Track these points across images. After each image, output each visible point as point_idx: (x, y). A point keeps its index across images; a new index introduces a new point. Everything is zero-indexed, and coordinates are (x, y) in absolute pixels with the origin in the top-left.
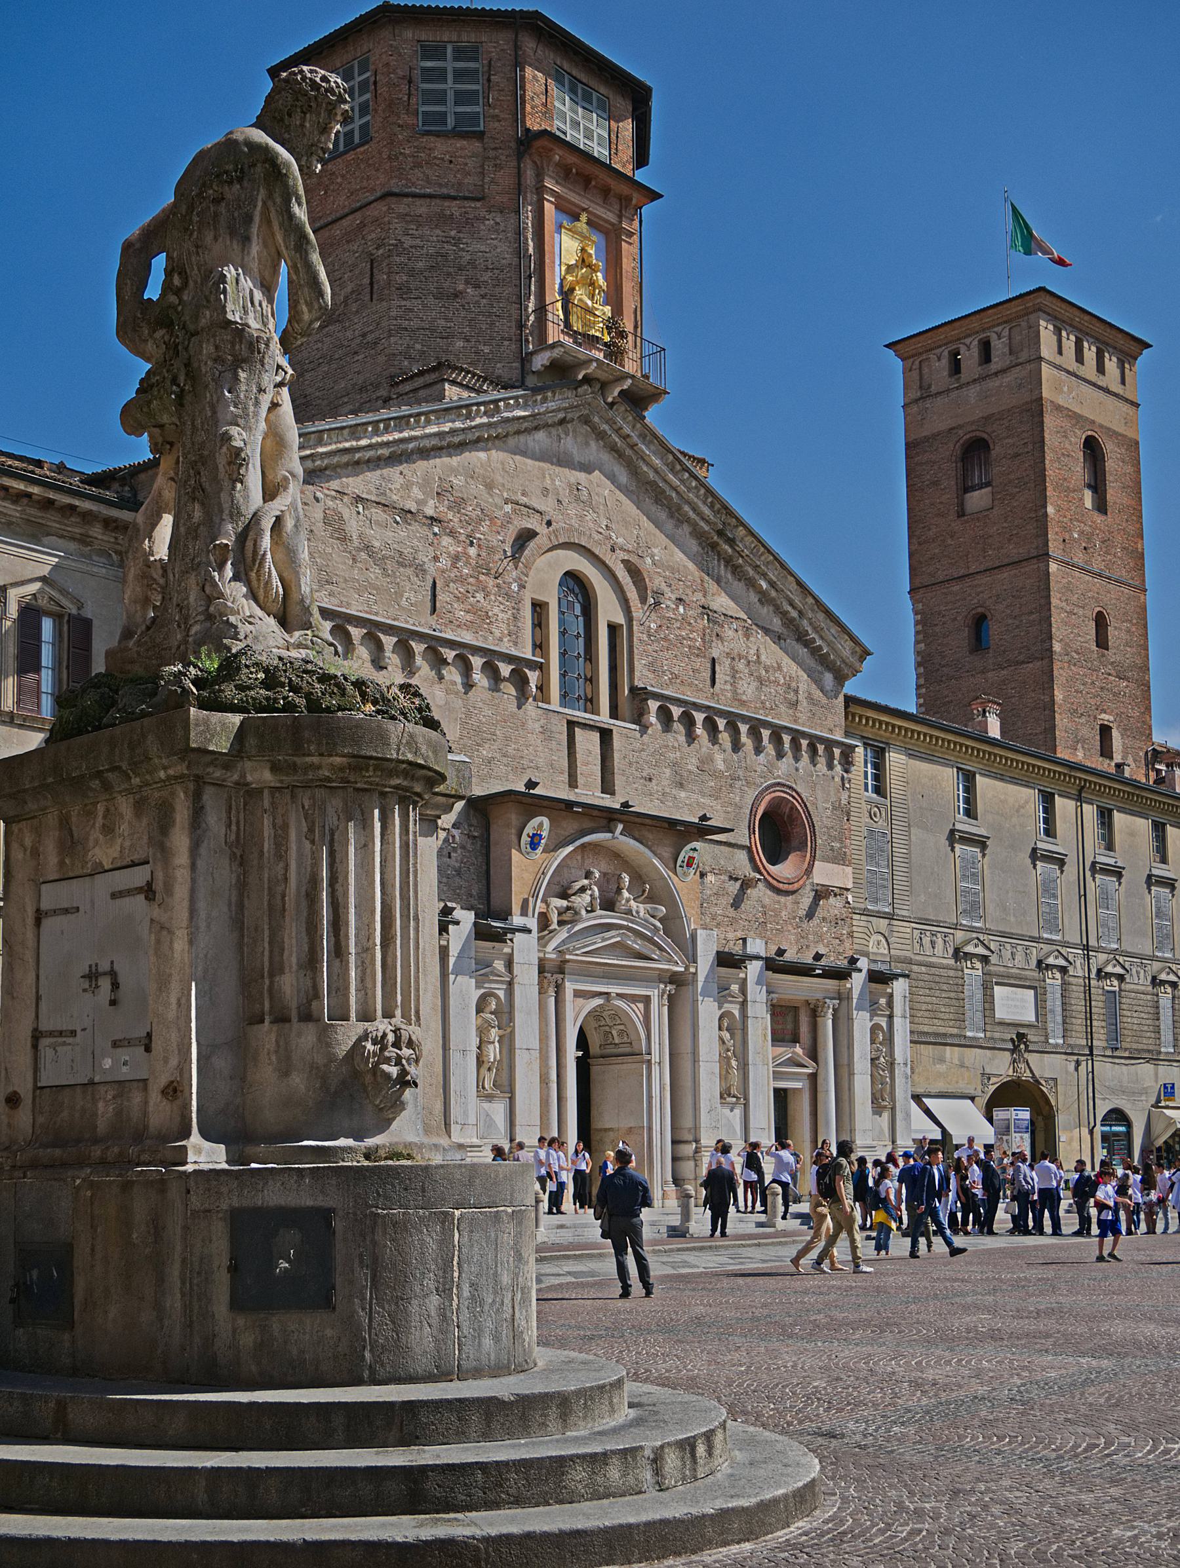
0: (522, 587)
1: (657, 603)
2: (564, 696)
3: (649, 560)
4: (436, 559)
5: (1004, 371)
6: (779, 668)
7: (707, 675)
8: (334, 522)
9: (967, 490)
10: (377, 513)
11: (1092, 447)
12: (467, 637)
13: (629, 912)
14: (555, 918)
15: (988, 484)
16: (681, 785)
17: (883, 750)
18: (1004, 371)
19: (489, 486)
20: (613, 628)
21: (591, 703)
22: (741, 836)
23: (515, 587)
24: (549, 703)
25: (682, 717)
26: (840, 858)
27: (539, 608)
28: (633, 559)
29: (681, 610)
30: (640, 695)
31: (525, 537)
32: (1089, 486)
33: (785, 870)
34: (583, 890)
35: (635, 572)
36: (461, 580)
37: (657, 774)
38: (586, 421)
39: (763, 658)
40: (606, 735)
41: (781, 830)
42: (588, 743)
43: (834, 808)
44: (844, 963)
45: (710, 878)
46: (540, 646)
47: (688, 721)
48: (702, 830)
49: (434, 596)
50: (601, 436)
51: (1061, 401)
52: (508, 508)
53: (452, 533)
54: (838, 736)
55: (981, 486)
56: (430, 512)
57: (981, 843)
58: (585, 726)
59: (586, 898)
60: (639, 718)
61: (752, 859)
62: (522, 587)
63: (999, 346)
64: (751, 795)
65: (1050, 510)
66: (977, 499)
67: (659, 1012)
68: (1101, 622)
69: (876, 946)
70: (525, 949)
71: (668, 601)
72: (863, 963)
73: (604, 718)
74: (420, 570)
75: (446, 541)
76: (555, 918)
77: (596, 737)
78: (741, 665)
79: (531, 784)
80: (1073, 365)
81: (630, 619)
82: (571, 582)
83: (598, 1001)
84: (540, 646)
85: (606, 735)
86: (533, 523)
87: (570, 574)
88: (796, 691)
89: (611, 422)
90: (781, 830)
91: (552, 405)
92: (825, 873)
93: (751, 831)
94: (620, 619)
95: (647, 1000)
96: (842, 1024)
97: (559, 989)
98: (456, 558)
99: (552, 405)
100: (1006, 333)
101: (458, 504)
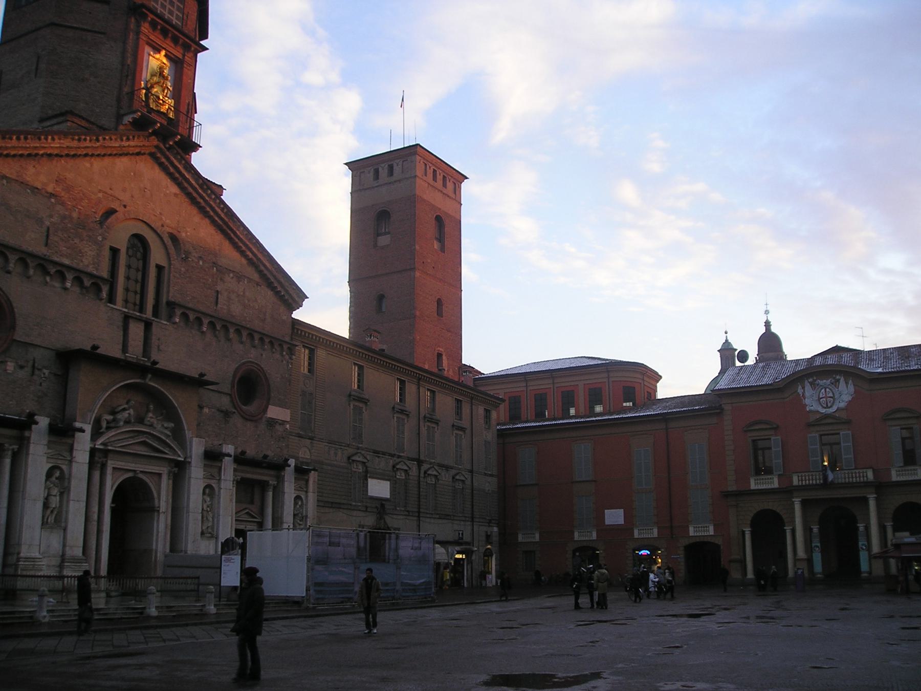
0: (104, 238)
1: (187, 258)
2: (126, 301)
4: (51, 216)
5: (399, 181)
6: (256, 301)
9: (379, 235)
11: (438, 219)
12: (66, 262)
13: (151, 425)
14: (104, 425)
15: (389, 233)
17: (313, 350)
18: (399, 181)
20: (160, 268)
21: (142, 309)
22: (226, 388)
23: (100, 238)
24: (115, 304)
25: (193, 318)
26: (282, 405)
27: (114, 251)
28: (175, 232)
29: (201, 263)
30: (171, 305)
31: (111, 212)
32: (436, 239)
33: (252, 408)
34: (124, 409)
35: (174, 239)
37: (176, 350)
38: (152, 155)
39: (247, 294)
40: (148, 325)
41: (249, 386)
42: (136, 330)
45: (206, 410)
47: (199, 321)
48: (199, 382)
49: (48, 236)
50: (161, 165)
51: (425, 197)
52: (100, 195)
54: (287, 339)
55: (385, 234)
56: (50, 189)
57: (365, 401)
59: (126, 414)
60: (170, 318)
61: (232, 401)
62: (104, 238)
63: (397, 170)
65: (417, 247)
66: (384, 240)
67: (166, 484)
68: (439, 302)
69: (305, 454)
70: (83, 444)
72: (292, 462)
75: (59, 207)
76: (104, 425)
77: (141, 326)
80: (432, 182)
81: (170, 264)
82: (136, 241)
83: (130, 475)
85: (148, 325)
86: (115, 205)
87: (136, 236)
90: (249, 386)
91: (132, 143)
92: (273, 412)
93: (233, 387)
94: (164, 263)
95: (160, 475)
96: (278, 492)
97: (103, 467)
98: (64, 217)
100: (400, 163)
101: (69, 189)
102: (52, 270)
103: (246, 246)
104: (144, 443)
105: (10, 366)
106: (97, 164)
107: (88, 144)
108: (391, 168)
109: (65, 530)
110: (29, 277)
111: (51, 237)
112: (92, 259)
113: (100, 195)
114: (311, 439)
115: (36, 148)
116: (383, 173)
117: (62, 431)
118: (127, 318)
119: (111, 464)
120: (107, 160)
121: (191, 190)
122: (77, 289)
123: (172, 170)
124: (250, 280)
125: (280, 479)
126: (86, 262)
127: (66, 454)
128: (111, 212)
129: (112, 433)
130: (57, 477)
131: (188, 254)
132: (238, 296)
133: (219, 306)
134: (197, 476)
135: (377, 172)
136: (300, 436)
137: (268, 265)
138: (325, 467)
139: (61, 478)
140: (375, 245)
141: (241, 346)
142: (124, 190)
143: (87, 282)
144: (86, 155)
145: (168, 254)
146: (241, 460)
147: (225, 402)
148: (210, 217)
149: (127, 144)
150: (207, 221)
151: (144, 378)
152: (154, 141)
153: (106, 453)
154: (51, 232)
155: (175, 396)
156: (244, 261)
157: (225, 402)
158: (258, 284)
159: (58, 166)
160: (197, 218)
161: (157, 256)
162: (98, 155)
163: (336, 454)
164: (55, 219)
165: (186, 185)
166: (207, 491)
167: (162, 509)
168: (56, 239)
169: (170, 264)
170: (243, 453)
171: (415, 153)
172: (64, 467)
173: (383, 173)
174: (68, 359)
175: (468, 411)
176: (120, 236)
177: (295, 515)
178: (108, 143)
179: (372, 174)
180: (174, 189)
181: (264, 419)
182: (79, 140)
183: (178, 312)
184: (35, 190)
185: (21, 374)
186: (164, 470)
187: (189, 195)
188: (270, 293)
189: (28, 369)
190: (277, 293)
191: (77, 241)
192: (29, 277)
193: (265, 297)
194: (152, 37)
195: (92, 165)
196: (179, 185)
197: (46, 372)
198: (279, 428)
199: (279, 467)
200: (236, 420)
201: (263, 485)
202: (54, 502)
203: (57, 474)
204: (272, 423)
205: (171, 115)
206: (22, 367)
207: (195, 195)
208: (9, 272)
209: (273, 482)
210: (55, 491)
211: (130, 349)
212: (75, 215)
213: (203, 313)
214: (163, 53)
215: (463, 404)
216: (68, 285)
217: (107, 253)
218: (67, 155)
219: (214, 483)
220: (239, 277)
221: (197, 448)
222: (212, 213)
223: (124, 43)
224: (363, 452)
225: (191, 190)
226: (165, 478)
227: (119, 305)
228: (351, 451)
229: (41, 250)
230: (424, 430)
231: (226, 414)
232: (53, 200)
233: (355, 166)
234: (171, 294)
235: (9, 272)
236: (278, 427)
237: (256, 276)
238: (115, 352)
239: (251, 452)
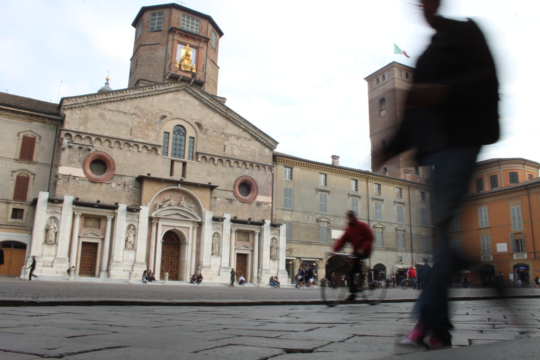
0: (160, 129)
3: (204, 122)
4: (133, 123)
6: (249, 147)
7: (223, 149)
8: (102, 116)
10: (116, 113)
16: (210, 176)
19: (152, 106)
23: (158, 129)
26: (266, 195)
31: (164, 117)
35: (199, 125)
36: (140, 127)
38: (185, 90)
39: (243, 145)
40: (184, 164)
41: (246, 186)
43: (265, 182)
44: (261, 221)
45: (218, 199)
46: (166, 142)
52: (158, 111)
53: (139, 117)
56: (132, 112)
58: (178, 161)
62: (160, 129)
63: (386, 76)
64: (234, 179)
71: (210, 132)
73: (186, 159)
74: (127, 125)
75: (136, 119)
77: (181, 164)
78: (235, 147)
79: (149, 175)
81: (197, 136)
84: (166, 142)
85: (184, 164)
88: (255, 153)
89: (192, 90)
90: (246, 186)
94: (194, 135)
95: (189, 228)
97: (157, 225)
98: (140, 122)
99: (171, 87)
101: (141, 110)
102: (132, 144)
103: (240, 123)
104: (177, 214)
105: (114, 185)
106: (156, 98)
107: (148, 90)
108: (384, 76)
109: (136, 251)
110: (121, 149)
111: (133, 131)
112: (154, 137)
113: (158, 111)
114: (292, 211)
115: (123, 96)
116: (381, 79)
117: (133, 210)
118: (172, 162)
119: (161, 223)
120: (161, 96)
121: (206, 102)
122: (145, 151)
123: (195, 95)
124: (245, 138)
125: (262, 230)
126: (151, 140)
127: (137, 220)
128: (164, 117)
129: (161, 210)
130: (132, 228)
131: (207, 130)
132: (238, 146)
133: (226, 152)
134: (208, 229)
135: (378, 79)
136: (283, 210)
137: (253, 130)
138: (301, 224)
139: (134, 229)
140: (380, 116)
141: (239, 169)
142: (170, 107)
143: (150, 148)
144: (149, 96)
145: (196, 132)
146: (234, 221)
147: (230, 195)
148: (219, 112)
149: (168, 87)
150: (218, 114)
151: (178, 186)
152: (183, 84)
153: (158, 219)
154: (133, 129)
155: (195, 193)
156: (241, 130)
157: (230, 195)
158: (250, 140)
159: (135, 102)
160: (211, 114)
161: (190, 132)
162: (155, 95)
163: (308, 218)
164: (135, 123)
165: (203, 100)
166: (216, 235)
167: (190, 242)
168: (135, 132)
169: (197, 136)
170: (235, 218)
171: (393, 66)
172: (135, 225)
173: (381, 79)
174: (140, 180)
175: (407, 193)
176: (170, 126)
177: (271, 247)
178: (158, 89)
179: (376, 81)
180: (197, 102)
181: (255, 202)
182: (143, 90)
183: (200, 156)
184: (125, 113)
185: (119, 188)
186: (191, 226)
187: (206, 104)
188: (258, 143)
189: (122, 186)
190: (262, 143)
191: (146, 131)
192: (121, 149)
193: (255, 146)
194: (180, 40)
195: (153, 99)
196: (200, 100)
197: (131, 186)
198: (264, 207)
199: (261, 224)
200: (237, 203)
201: (253, 233)
202: (131, 239)
203: (132, 227)
204: (259, 204)
205: (194, 71)
206: (119, 185)
207: (208, 104)
208: (112, 147)
209: (257, 231)
210: (131, 235)
211: (175, 174)
212: (145, 121)
213: (215, 156)
214: (188, 45)
215: (403, 190)
216: (140, 150)
217: (162, 135)
218: (140, 97)
219: (220, 232)
220: (238, 138)
221: (208, 216)
222: (219, 111)
223: (167, 45)
224: (327, 217)
225: (206, 102)
226: (191, 229)
227: (170, 156)
228: (318, 216)
229: (128, 137)
230: (372, 204)
231: (231, 201)
232: (134, 116)
233: (369, 79)
234: (198, 149)
235: (112, 147)
236: (263, 205)
237: (249, 136)
238: (167, 176)
239: (240, 218)
